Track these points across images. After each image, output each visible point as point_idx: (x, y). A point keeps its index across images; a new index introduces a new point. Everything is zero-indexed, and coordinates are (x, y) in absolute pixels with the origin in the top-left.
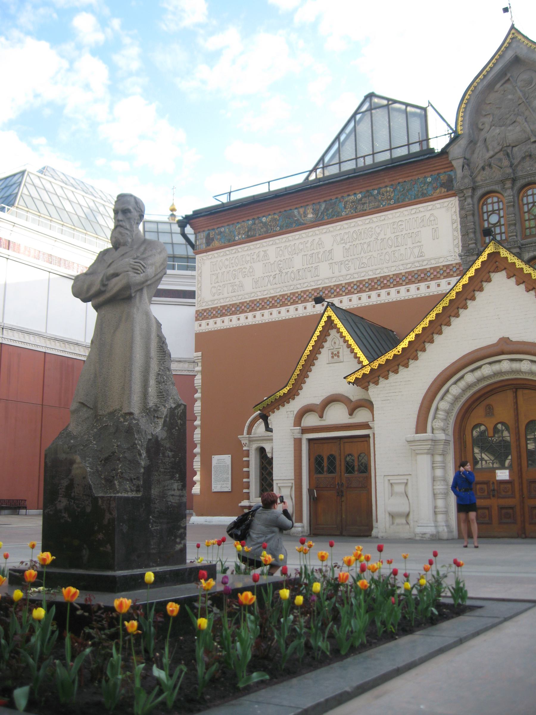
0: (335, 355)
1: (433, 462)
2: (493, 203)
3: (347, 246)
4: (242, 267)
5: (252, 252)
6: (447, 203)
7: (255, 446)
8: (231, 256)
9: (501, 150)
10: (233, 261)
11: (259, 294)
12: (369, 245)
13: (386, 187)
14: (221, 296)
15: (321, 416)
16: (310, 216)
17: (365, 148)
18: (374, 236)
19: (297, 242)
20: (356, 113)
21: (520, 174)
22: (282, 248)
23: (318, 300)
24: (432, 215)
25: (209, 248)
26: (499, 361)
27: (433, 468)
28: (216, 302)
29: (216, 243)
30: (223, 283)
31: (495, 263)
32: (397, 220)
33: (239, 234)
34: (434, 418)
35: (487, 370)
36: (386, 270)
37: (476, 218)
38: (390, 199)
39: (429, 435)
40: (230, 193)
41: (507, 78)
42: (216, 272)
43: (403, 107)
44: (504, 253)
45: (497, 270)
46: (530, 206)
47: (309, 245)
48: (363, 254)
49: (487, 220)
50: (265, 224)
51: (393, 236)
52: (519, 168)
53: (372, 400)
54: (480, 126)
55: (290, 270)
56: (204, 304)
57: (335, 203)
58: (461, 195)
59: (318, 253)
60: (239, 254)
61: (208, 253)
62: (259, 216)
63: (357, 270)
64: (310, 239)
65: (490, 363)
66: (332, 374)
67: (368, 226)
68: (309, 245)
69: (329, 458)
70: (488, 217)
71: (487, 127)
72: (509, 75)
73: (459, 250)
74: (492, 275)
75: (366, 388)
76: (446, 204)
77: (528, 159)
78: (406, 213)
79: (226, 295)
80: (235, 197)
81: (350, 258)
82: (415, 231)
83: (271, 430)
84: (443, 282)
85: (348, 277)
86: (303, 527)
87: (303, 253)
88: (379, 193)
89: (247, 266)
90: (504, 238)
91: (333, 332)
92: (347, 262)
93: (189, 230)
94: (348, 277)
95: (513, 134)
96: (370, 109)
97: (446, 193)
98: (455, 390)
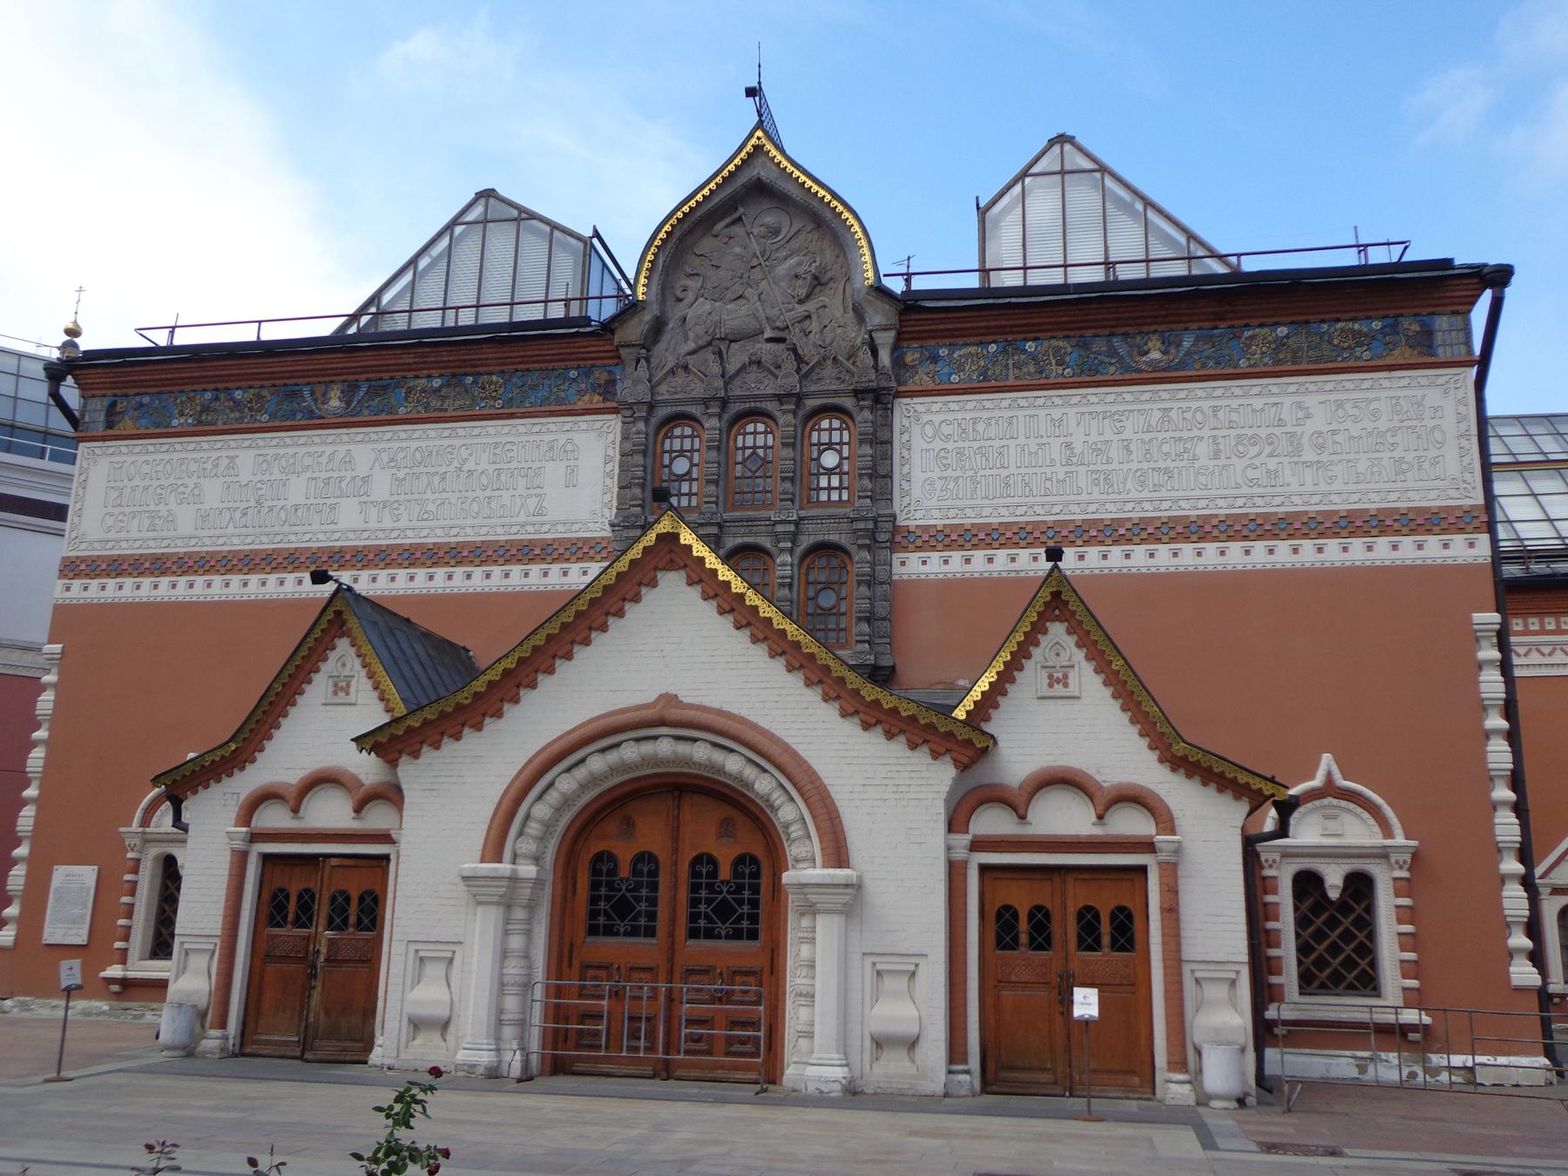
0: (342, 689)
1: (507, 921)
2: (683, 437)
3: (401, 474)
5: (205, 455)
7: (154, 851)
8: (159, 457)
9: (709, 344)
10: (160, 468)
13: (490, 374)
14: (123, 535)
15: (295, 810)
16: (335, 403)
17: (463, 294)
18: (456, 464)
20: (455, 222)
21: (738, 392)
23: (319, 577)
24: (569, 441)
25: (111, 432)
26: (656, 738)
27: (506, 933)
28: (110, 545)
29: (127, 425)
31: (669, 553)
32: (504, 440)
33: (182, 414)
34: (520, 834)
35: (630, 752)
36: (469, 531)
37: (649, 461)
38: (495, 399)
39: (504, 868)
40: (174, 328)
41: (736, 216)
43: (548, 229)
44: (687, 537)
45: (671, 566)
46: (748, 452)
47: (324, 459)
48: (429, 495)
49: (669, 466)
50: (237, 405)
52: (737, 382)
53: (404, 786)
54: (679, 294)
55: (281, 503)
56: (83, 546)
57: (385, 387)
58: (628, 413)
59: (341, 479)
60: (177, 456)
62: (230, 385)
63: (415, 524)
64: (329, 449)
65: (638, 740)
66: (330, 725)
67: (447, 442)
68: (324, 459)
69: (300, 897)
70: (672, 460)
71: (690, 296)
72: (741, 210)
73: (611, 514)
74: (659, 575)
75: (393, 763)
76: (598, 425)
77: (754, 367)
78: (522, 429)
79: (134, 534)
80: (183, 338)
81: (402, 498)
82: (535, 465)
83: (185, 829)
84: (575, 568)
85: (395, 534)
86: (226, 1038)
89: (191, 483)
90: (694, 503)
91: (343, 644)
93: (70, 392)
94: (395, 534)
95: (735, 316)
96: (484, 221)
97: (601, 405)
98: (566, 784)
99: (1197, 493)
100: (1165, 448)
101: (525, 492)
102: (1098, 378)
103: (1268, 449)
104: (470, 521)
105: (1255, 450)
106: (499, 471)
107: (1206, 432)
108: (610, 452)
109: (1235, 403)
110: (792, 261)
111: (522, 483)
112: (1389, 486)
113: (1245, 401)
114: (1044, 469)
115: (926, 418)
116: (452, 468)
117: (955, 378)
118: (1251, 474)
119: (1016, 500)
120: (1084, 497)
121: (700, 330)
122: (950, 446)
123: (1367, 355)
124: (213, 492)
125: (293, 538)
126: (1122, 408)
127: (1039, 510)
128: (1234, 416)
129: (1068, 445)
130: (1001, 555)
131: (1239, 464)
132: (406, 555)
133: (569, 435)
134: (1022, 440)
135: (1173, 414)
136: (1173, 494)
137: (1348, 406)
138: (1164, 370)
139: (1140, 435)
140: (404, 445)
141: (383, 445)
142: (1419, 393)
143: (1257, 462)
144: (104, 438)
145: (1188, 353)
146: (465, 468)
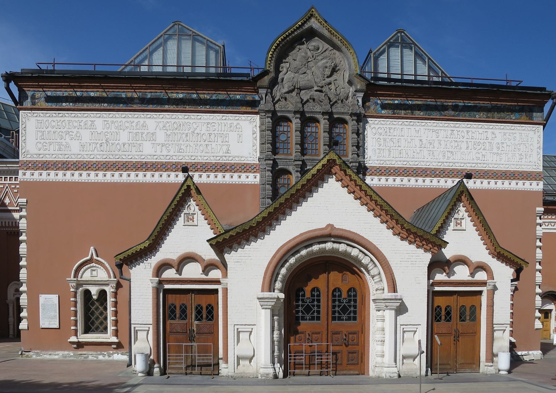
3: (169, 133)
4: (70, 130)
5: (80, 119)
6: (250, 118)
11: (85, 156)
12: (187, 136)
14: (47, 152)
18: (191, 130)
19: (124, 120)
22: (109, 122)
28: (41, 156)
30: (49, 141)
36: (199, 158)
42: (41, 129)
47: (134, 124)
48: (181, 142)
51: (207, 133)
55: (117, 142)
56: (29, 156)
59: (142, 133)
61: (33, 112)
63: (176, 154)
64: (136, 120)
67: (187, 121)
68: (134, 124)
76: (249, 118)
81: (170, 142)
82: (225, 133)
87: (128, 130)
89: (75, 131)
92: (167, 146)
94: (168, 157)
95: (303, 80)
99: (461, 161)
100: (452, 144)
101: (221, 144)
102: (431, 117)
103: (483, 147)
104: (199, 154)
105: (479, 147)
106: (210, 135)
107: (465, 140)
108: (255, 129)
109: (473, 130)
110: (324, 61)
111: (220, 140)
112: (517, 163)
113: (477, 130)
114: (413, 148)
115: (372, 126)
116: (190, 132)
117: (383, 112)
118: (478, 155)
119: (404, 159)
120: (425, 160)
121: (291, 84)
122: (381, 137)
123: (514, 118)
124: (86, 135)
125: (124, 157)
126: (438, 128)
127: (411, 163)
128: (473, 135)
129: (421, 140)
130: (398, 179)
131: (474, 152)
132: (174, 166)
133: (238, 122)
134: (405, 137)
135: (455, 132)
136: (454, 161)
137: (507, 135)
138: (453, 116)
139: (444, 139)
140: (169, 120)
141: (160, 120)
142: (528, 132)
143: (479, 151)
144: (31, 109)
146: (196, 132)
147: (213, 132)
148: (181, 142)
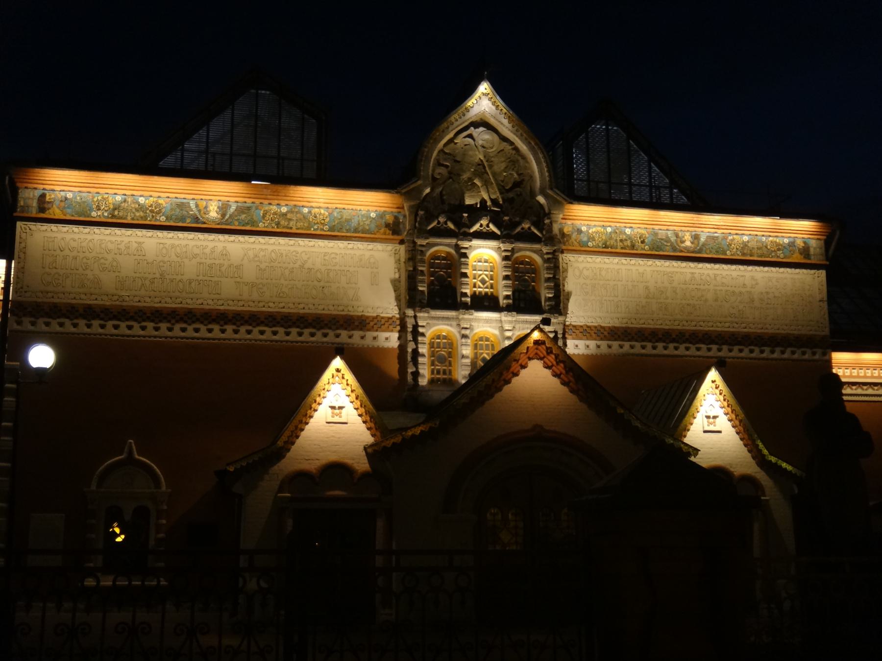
33: (99, 209)
88: (310, 212)
138: (693, 252)
145: (704, 245)
147: (333, 268)
148: (282, 281)
